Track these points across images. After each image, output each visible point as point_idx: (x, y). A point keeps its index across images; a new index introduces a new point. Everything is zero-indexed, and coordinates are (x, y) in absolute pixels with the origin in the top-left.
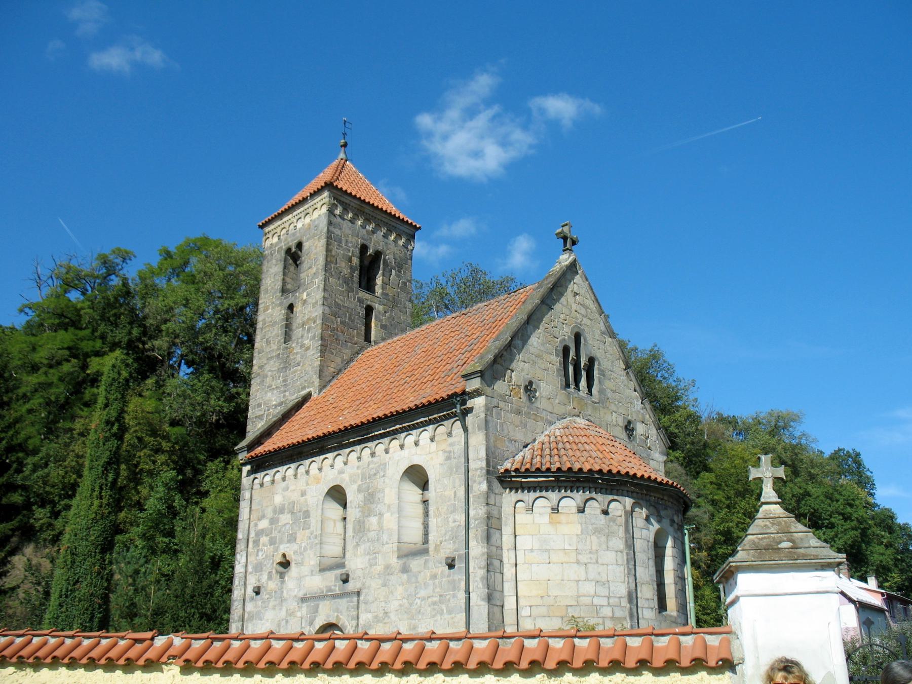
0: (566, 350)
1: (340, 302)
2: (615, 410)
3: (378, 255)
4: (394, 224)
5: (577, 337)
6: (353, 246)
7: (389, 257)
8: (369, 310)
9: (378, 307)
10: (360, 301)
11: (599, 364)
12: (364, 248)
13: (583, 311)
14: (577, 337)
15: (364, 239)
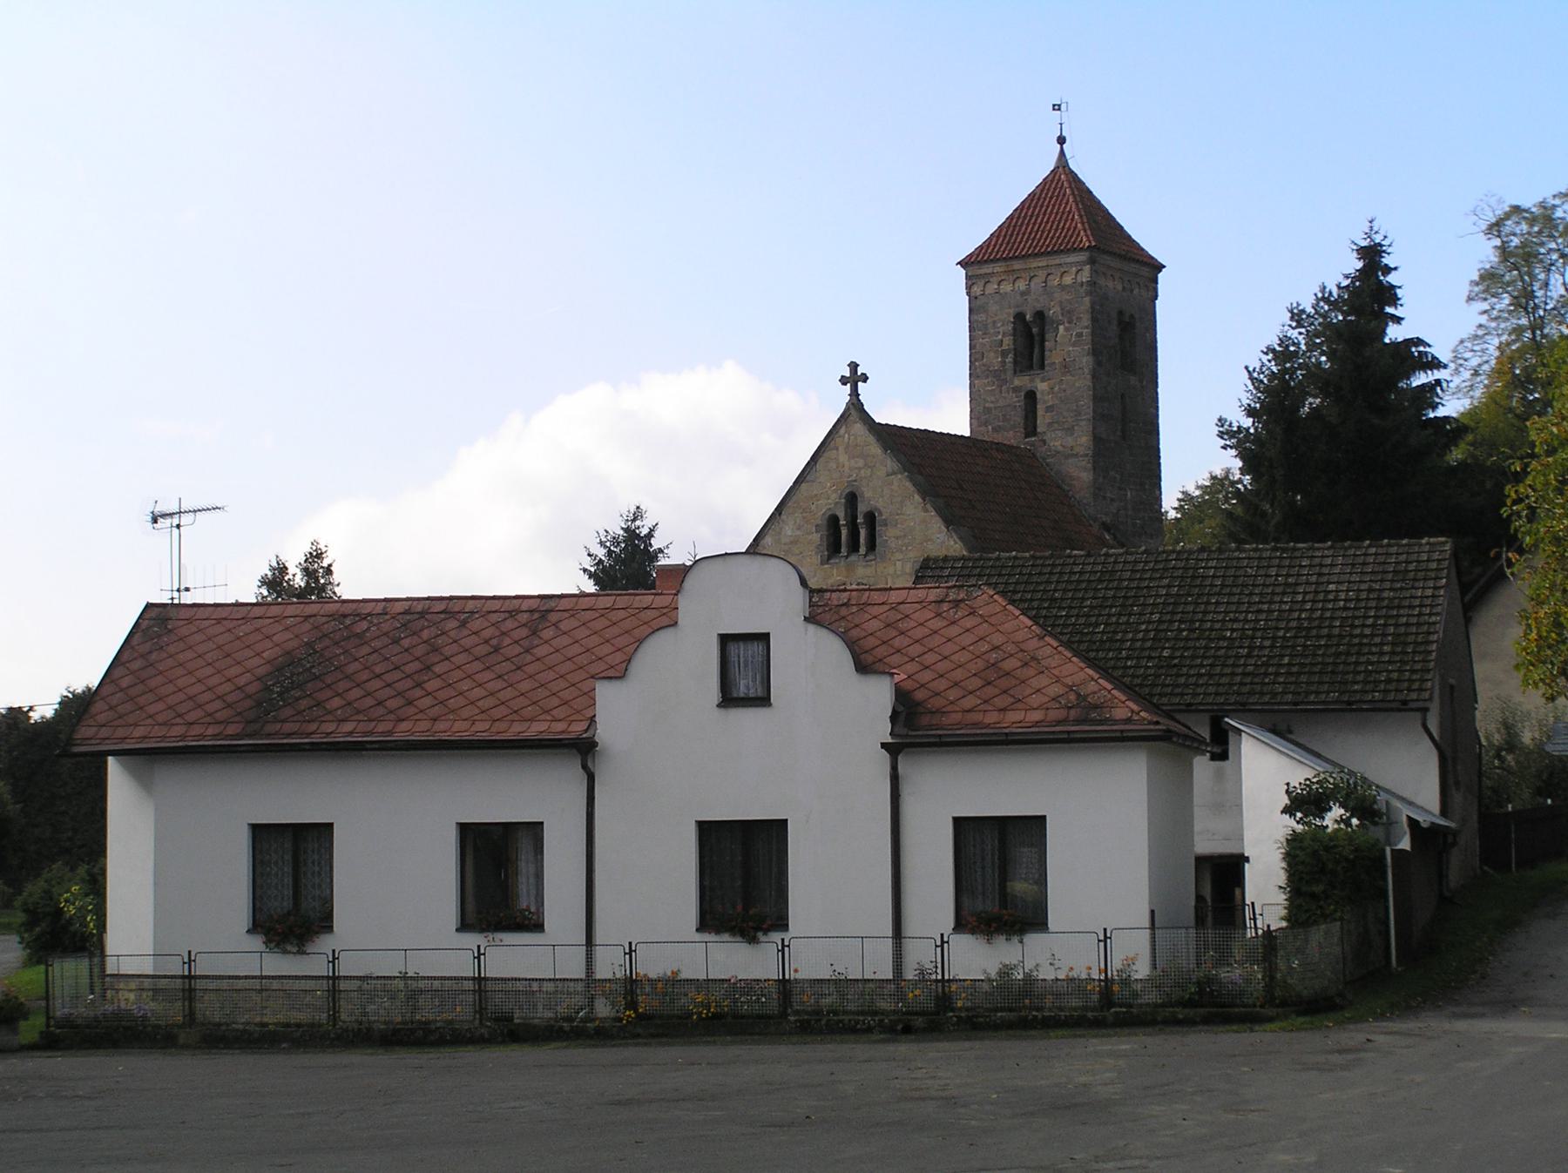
0: (833, 521)
1: (992, 405)
2: (901, 557)
3: (1040, 315)
4: (1057, 261)
5: (852, 499)
6: (1003, 325)
7: (1053, 311)
8: (1031, 396)
9: (1041, 387)
10: (1016, 390)
11: (880, 514)
12: (1020, 317)
13: (861, 463)
14: (852, 499)
15: (1018, 306)
